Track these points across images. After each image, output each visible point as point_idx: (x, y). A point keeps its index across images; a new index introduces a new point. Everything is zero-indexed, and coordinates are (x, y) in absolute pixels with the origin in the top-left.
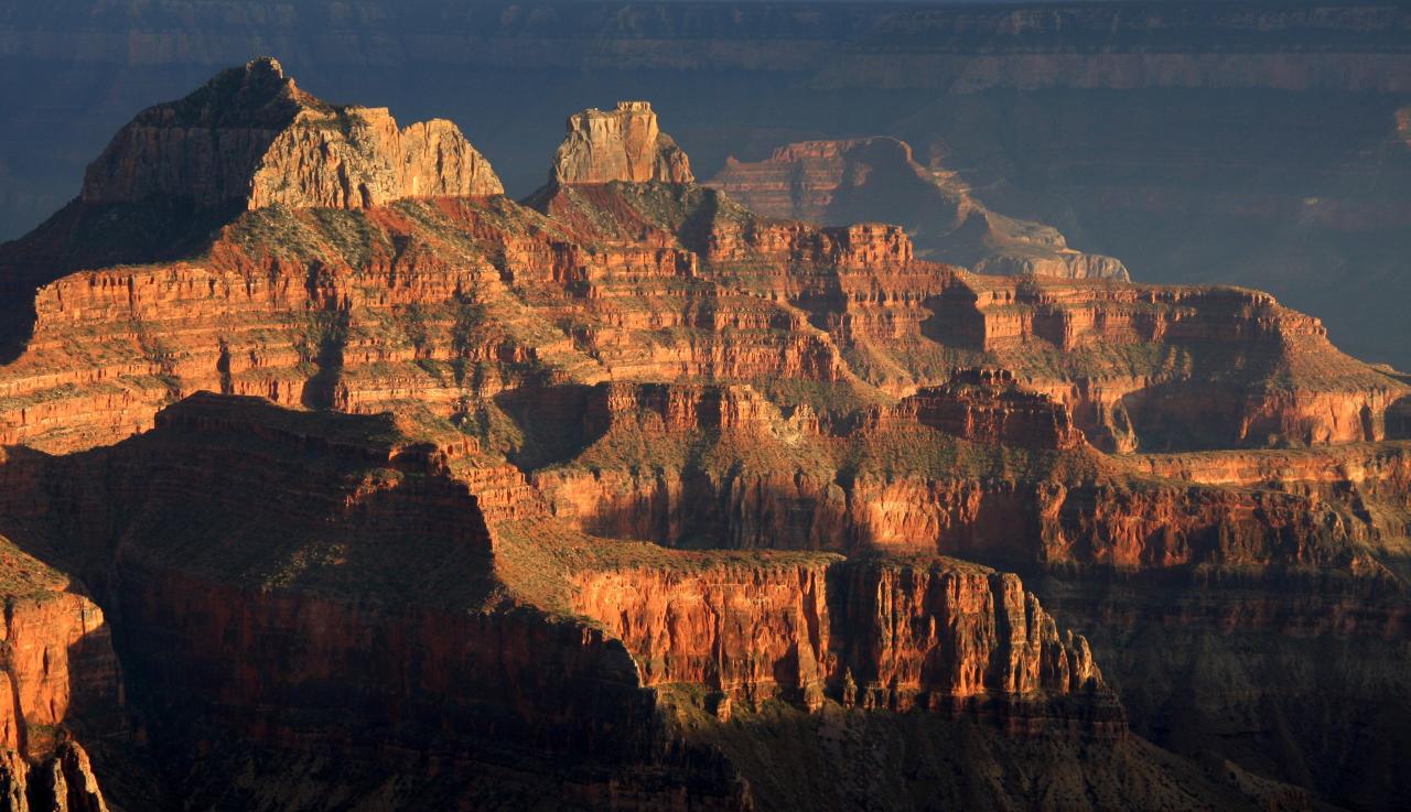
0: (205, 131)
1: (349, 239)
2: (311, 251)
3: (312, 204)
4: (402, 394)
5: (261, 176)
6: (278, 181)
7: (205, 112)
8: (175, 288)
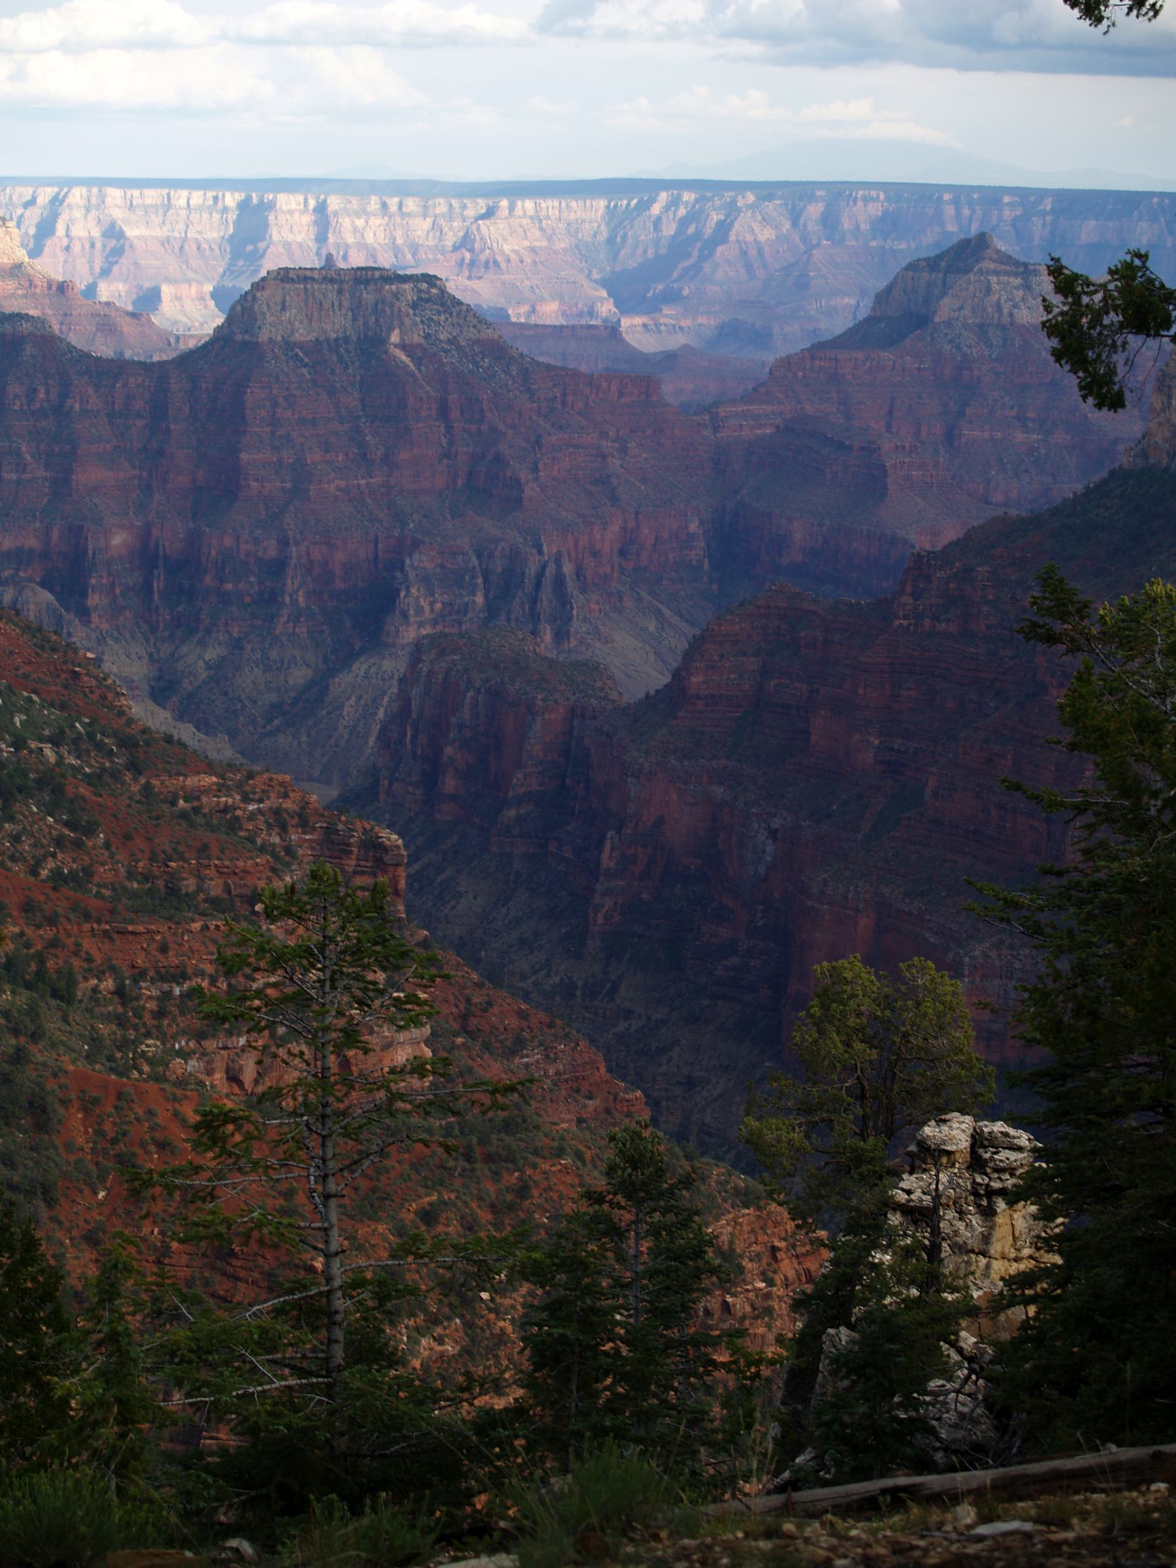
0: (941, 275)
1: (995, 343)
2: (965, 349)
3: (978, 321)
4: (999, 435)
5: (946, 301)
6: (958, 305)
7: (943, 264)
8: (868, 364)
